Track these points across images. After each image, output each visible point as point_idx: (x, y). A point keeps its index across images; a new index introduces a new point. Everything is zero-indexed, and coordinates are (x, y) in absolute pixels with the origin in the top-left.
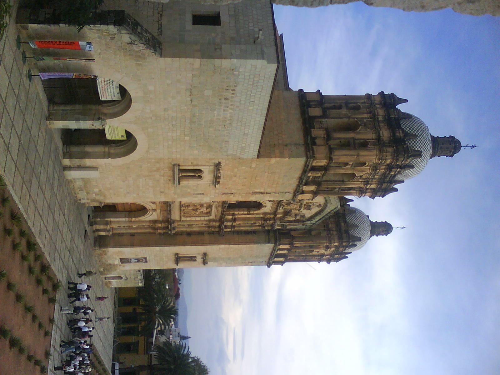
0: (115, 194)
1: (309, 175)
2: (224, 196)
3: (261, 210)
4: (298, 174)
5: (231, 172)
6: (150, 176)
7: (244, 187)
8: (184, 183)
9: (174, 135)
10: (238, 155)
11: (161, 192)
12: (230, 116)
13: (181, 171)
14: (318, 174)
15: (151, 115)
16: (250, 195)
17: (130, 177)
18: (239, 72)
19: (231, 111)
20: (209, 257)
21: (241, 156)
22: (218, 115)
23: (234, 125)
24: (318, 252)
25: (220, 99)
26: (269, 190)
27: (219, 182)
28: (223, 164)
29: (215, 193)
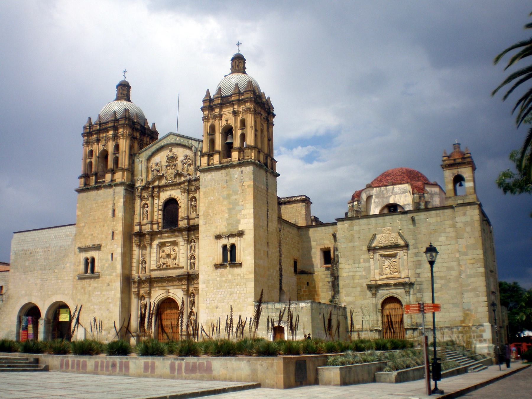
0: (109, 320)
1: (93, 184)
2: (115, 238)
3: (176, 198)
4: (94, 193)
5: (88, 238)
6: (89, 293)
7: (106, 225)
8: (96, 269)
9: (53, 279)
10: (72, 237)
11: (109, 285)
12: (42, 249)
13: (86, 271)
14: (92, 179)
15: (39, 293)
16: (115, 218)
17: (90, 307)
18: (17, 250)
19: (38, 250)
20: (226, 230)
21: (73, 235)
22: (41, 255)
23: (48, 245)
24: (227, 121)
25: (31, 256)
26: (110, 206)
27: (98, 245)
28: (80, 245)
29: (111, 244)
